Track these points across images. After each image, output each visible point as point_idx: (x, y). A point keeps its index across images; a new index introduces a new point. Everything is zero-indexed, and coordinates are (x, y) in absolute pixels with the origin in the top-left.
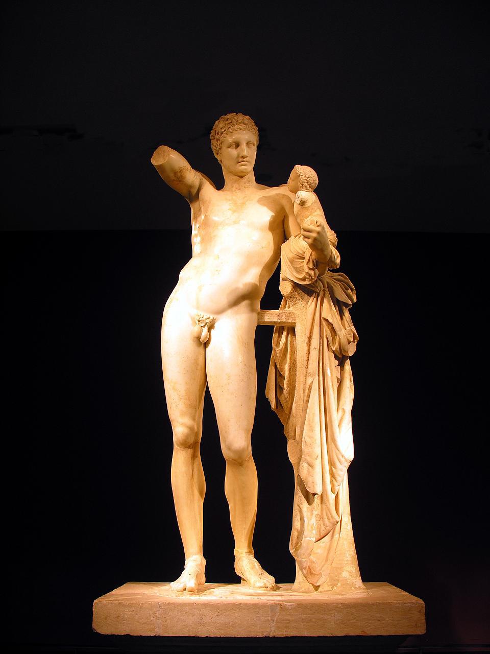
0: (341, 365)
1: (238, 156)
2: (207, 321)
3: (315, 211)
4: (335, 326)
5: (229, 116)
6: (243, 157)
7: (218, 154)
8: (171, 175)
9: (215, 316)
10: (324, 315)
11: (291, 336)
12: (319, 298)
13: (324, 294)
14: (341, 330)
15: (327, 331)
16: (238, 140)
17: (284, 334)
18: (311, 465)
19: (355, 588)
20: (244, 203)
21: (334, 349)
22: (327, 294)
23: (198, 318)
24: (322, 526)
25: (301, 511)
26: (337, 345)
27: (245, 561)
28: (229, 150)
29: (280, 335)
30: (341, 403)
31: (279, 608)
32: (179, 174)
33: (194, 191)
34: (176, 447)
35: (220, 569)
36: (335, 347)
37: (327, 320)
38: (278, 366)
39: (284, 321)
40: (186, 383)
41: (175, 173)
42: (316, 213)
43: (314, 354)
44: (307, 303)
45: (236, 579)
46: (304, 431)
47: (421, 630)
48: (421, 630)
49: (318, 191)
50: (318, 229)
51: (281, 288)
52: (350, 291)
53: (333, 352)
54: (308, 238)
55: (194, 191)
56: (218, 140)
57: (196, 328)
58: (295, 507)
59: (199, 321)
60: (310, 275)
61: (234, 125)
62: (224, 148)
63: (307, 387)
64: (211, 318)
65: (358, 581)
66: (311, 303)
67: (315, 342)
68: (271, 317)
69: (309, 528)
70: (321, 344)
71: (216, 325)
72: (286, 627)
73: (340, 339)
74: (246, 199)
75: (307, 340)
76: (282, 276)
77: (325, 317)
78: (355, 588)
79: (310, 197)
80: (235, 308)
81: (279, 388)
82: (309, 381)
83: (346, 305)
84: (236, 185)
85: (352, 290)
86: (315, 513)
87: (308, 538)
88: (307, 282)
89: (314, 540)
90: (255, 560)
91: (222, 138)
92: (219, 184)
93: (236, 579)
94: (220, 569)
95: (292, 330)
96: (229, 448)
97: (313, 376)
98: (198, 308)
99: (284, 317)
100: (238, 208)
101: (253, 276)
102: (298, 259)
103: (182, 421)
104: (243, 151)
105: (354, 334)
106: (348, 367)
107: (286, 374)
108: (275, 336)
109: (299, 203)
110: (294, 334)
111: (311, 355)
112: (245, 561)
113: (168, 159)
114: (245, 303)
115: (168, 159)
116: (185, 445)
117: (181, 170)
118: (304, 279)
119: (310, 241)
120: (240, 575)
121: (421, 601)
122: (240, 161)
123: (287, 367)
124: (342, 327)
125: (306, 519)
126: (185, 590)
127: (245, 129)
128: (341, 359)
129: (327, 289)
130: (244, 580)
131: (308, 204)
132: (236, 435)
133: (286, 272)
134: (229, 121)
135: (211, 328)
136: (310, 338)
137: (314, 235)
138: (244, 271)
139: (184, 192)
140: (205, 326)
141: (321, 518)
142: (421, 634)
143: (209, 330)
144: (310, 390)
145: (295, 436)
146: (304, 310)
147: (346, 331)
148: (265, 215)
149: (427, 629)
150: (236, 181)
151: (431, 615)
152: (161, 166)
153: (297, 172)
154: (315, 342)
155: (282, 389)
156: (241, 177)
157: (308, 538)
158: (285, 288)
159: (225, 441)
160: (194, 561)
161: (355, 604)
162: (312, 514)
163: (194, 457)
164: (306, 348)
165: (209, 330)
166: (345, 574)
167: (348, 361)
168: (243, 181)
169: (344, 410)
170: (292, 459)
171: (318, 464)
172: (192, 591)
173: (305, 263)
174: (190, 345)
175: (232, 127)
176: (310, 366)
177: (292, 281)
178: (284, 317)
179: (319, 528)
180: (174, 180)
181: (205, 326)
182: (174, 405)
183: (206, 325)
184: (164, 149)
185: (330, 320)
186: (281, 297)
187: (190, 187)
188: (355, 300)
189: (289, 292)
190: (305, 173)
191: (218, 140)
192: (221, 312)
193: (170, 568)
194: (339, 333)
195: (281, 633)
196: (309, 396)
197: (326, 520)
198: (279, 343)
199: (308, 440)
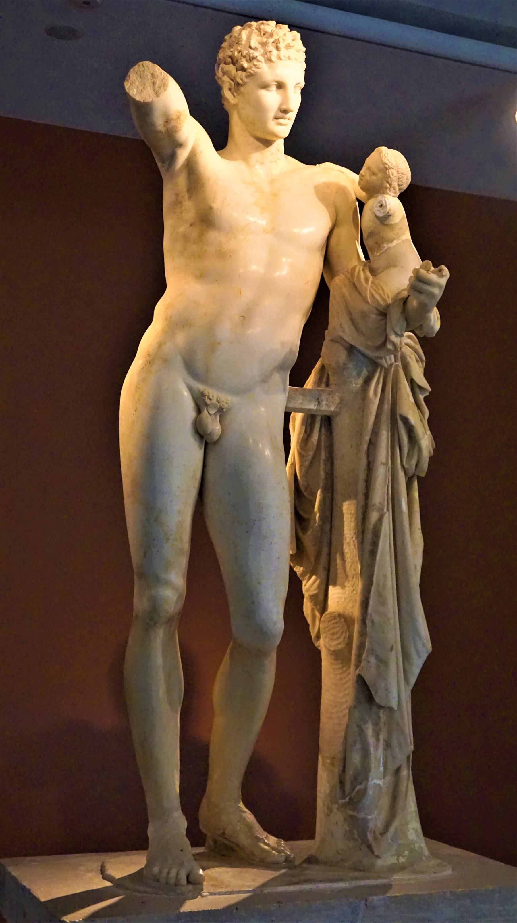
13: (396, 372)
28: (263, 93)
32: (173, 123)
37: (405, 421)
41: (167, 121)
46: (371, 603)
92: (220, 141)
117: (179, 117)
122: (278, 116)
153: (386, 161)
180: (161, 132)
190: (393, 162)
199: (376, 618)
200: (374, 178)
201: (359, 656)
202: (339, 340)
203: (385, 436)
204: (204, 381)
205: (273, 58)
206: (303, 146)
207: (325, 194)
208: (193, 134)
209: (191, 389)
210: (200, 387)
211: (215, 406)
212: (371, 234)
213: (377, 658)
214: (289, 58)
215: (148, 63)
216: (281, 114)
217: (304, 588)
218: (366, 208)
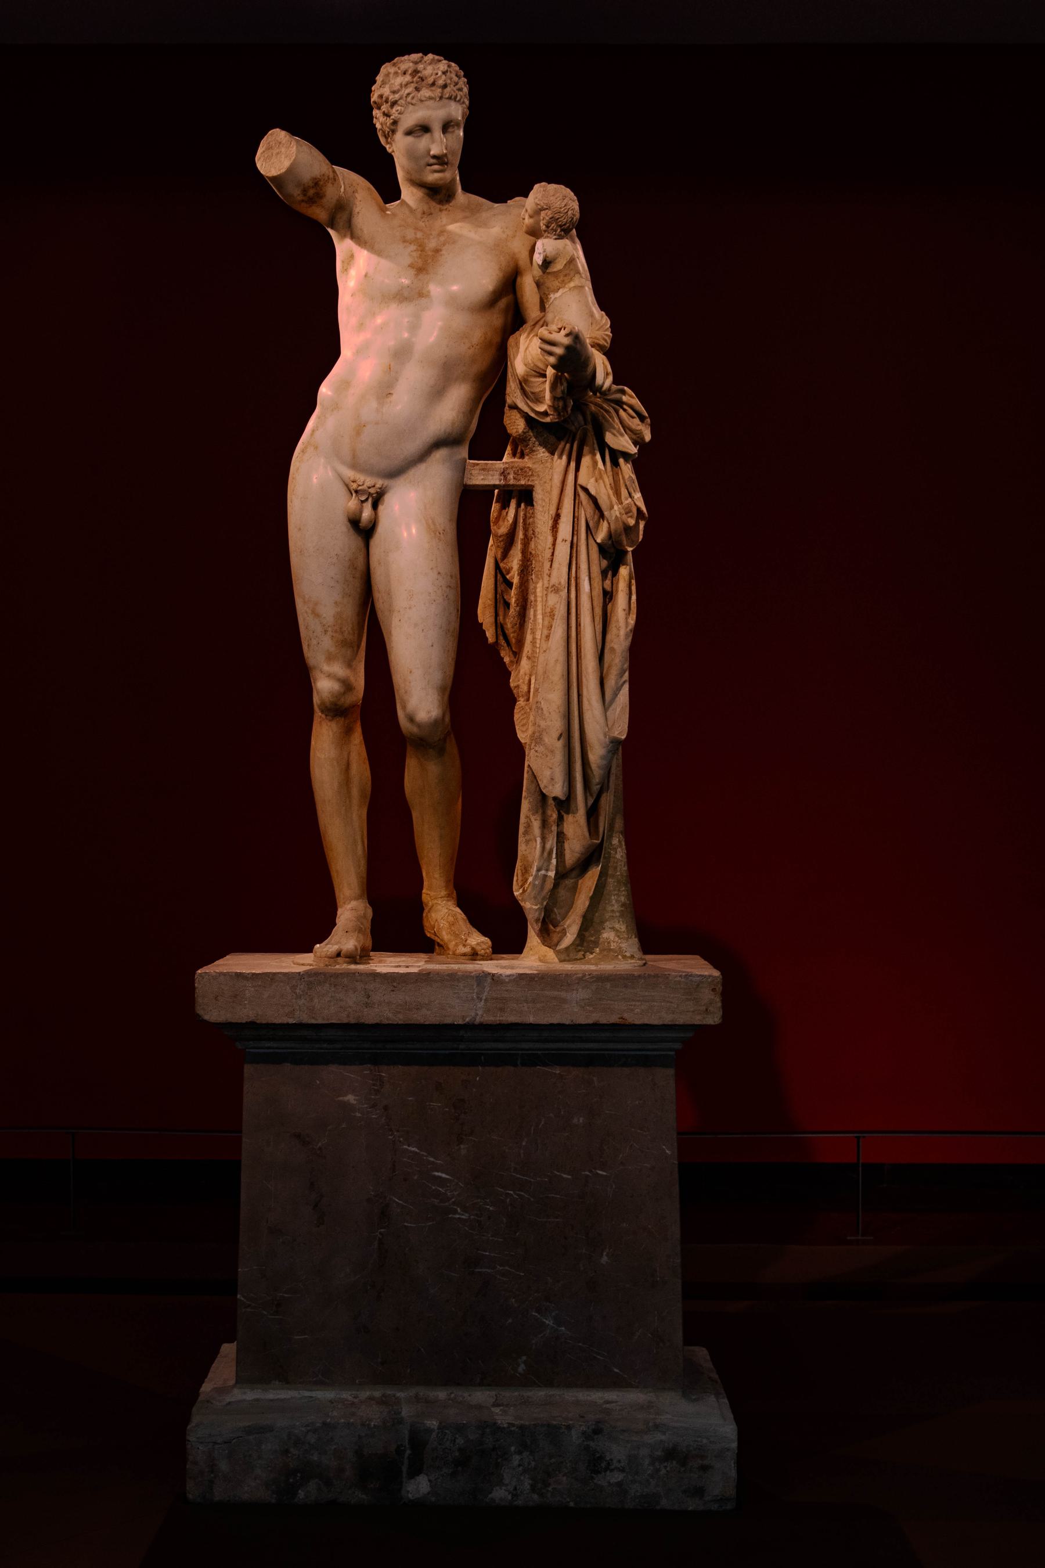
0: (611, 570)
2: (372, 491)
3: (571, 280)
4: (603, 502)
9: (386, 482)
10: (581, 481)
11: (527, 505)
14: (612, 507)
15: (586, 511)
17: (513, 504)
19: (624, 957)
20: (437, 251)
21: (599, 541)
23: (354, 486)
25: (529, 826)
27: (443, 914)
29: (505, 505)
30: (609, 637)
31: (489, 980)
34: (318, 714)
35: (398, 926)
36: (601, 536)
37: (586, 490)
38: (501, 565)
39: (512, 482)
40: (336, 603)
42: (572, 284)
43: (563, 551)
45: (423, 943)
50: (566, 341)
51: (507, 421)
52: (637, 421)
54: (550, 354)
57: (353, 503)
58: (523, 819)
59: (356, 492)
61: (417, 89)
63: (548, 610)
64: (378, 486)
65: (631, 946)
67: (565, 529)
68: (486, 474)
69: (546, 854)
70: (575, 531)
71: (387, 498)
72: (502, 1010)
74: (442, 239)
75: (551, 523)
76: (509, 401)
77: (584, 485)
78: (624, 957)
80: (422, 467)
81: (500, 603)
83: (626, 456)
85: (642, 418)
87: (543, 872)
89: (552, 874)
90: (458, 910)
92: (389, 192)
93: (423, 943)
94: (398, 926)
95: (526, 496)
96: (411, 719)
97: (556, 590)
98: (354, 466)
99: (511, 476)
102: (535, 376)
105: (639, 510)
107: (516, 581)
108: (495, 507)
109: (540, 263)
111: (556, 553)
112: (443, 914)
114: (441, 454)
116: (336, 710)
119: (552, 360)
120: (433, 937)
124: (614, 499)
126: (339, 955)
128: (611, 555)
129: (590, 427)
130: (439, 945)
131: (558, 266)
134: (408, 78)
136: (557, 516)
137: (559, 351)
138: (437, 393)
140: (367, 500)
142: (713, 1023)
143: (375, 506)
144: (552, 615)
145: (529, 692)
146: (548, 465)
149: (724, 1017)
154: (565, 529)
155: (507, 605)
157: (543, 872)
159: (404, 708)
160: (351, 911)
161: (611, 975)
163: (348, 731)
164: (550, 539)
165: (375, 506)
167: (630, 557)
169: (613, 650)
170: (523, 736)
172: (352, 958)
173: (547, 386)
174: (342, 540)
176: (554, 573)
178: (511, 476)
179: (561, 855)
181: (367, 500)
182: (314, 642)
183: (370, 500)
184: (277, 136)
186: (509, 436)
188: (648, 437)
189: (520, 431)
191: (387, 115)
192: (396, 473)
193: (310, 925)
194: (606, 513)
195: (492, 1018)
196: (550, 627)
198: (503, 519)
200: (531, 220)
202: (514, 407)
205: (414, 101)
211: (363, 492)
214: (431, 98)
216: (432, 161)
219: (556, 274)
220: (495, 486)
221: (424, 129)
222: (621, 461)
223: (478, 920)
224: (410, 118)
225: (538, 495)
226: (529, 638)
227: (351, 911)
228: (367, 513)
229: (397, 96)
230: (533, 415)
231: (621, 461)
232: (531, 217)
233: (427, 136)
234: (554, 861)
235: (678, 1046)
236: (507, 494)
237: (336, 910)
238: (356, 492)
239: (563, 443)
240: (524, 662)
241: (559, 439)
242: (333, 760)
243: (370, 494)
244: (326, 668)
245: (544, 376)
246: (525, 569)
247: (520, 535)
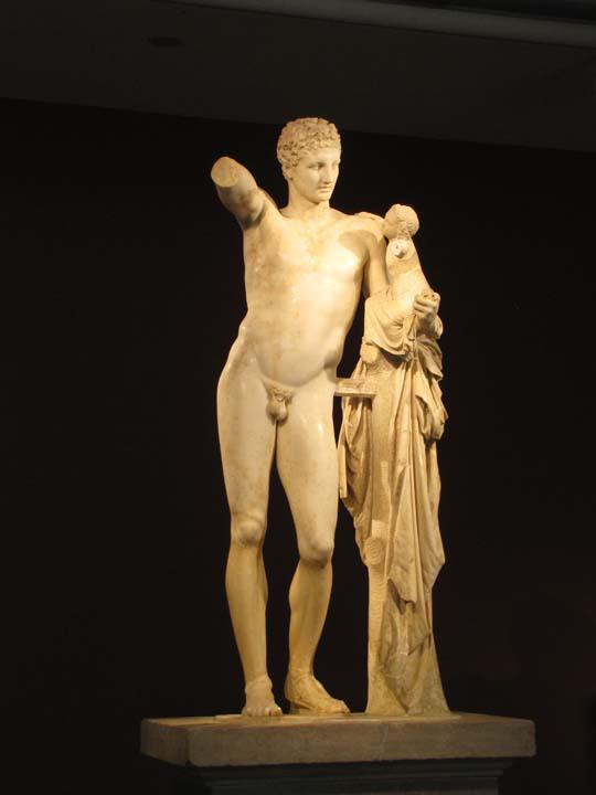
1: (321, 181)
5: (313, 122)
6: (327, 183)
7: (287, 168)
8: (237, 199)
12: (410, 370)
13: (415, 364)
16: (316, 151)
17: (360, 406)
18: (405, 569)
21: (424, 432)
22: (418, 363)
24: (414, 639)
26: (429, 428)
28: (310, 171)
33: (255, 216)
36: (427, 430)
37: (421, 399)
38: (350, 446)
41: (242, 197)
43: (404, 439)
44: (394, 373)
47: (531, 752)
48: (531, 752)
49: (418, 239)
51: (362, 352)
53: (423, 434)
55: (255, 216)
56: (294, 154)
60: (408, 346)
62: (302, 166)
63: (397, 476)
66: (400, 372)
71: (294, 399)
73: (433, 419)
77: (420, 395)
79: (408, 246)
82: (399, 469)
83: (436, 377)
84: (308, 213)
86: (407, 623)
88: (402, 353)
91: (301, 153)
92: (281, 200)
96: (314, 548)
99: (363, 389)
100: (318, 247)
101: (335, 342)
103: (250, 518)
104: (327, 173)
106: (434, 452)
110: (370, 407)
112: (306, 683)
113: (232, 175)
115: (232, 175)
116: (248, 542)
118: (399, 349)
121: (531, 722)
123: (360, 446)
125: (399, 631)
127: (331, 147)
129: (417, 358)
132: (317, 528)
133: (372, 333)
135: (288, 401)
138: (327, 333)
139: (242, 213)
141: (411, 628)
147: (438, 412)
148: (352, 263)
150: (310, 207)
151: (539, 737)
152: (228, 190)
156: (317, 204)
158: (368, 353)
159: (308, 540)
160: (259, 685)
162: (404, 625)
166: (434, 696)
167: (434, 445)
168: (318, 208)
171: (413, 572)
175: (317, 143)
177: (377, 346)
185: (425, 400)
187: (253, 211)
191: (294, 154)
197: (419, 632)
201: (389, 566)
203: (406, 409)
204: (274, 378)
206: (347, 199)
207: (357, 240)
208: (261, 200)
209: (264, 384)
210: (270, 382)
212: (391, 267)
213: (402, 567)
215: (227, 159)
217: (355, 523)
218: (391, 244)
219: (406, 262)
220: (348, 395)
221: (321, 165)
222: (434, 380)
223: (334, 692)
224: (312, 158)
225: (376, 403)
226: (369, 494)
227: (259, 685)
228: (282, 410)
229: (304, 144)
230: (386, 349)
231: (434, 380)
232: (390, 224)
233: (323, 169)
234: (407, 645)
235: (499, 773)
236: (355, 401)
237: (243, 684)
238: (276, 395)
239: (400, 369)
240: (366, 510)
241: (397, 366)
242: (245, 576)
243: (285, 398)
244: (250, 513)
245: (401, 325)
246: (368, 450)
247: (365, 427)
